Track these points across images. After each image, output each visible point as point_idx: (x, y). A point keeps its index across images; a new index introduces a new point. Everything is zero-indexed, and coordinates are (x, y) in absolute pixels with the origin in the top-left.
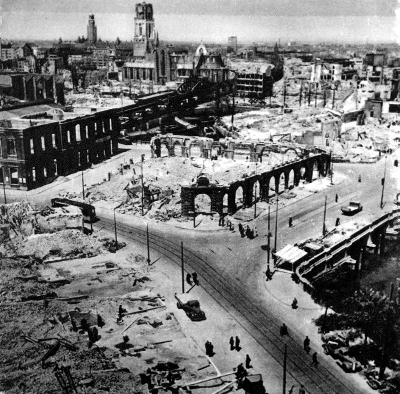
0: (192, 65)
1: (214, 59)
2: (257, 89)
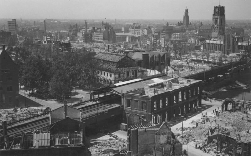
0: (247, 43)
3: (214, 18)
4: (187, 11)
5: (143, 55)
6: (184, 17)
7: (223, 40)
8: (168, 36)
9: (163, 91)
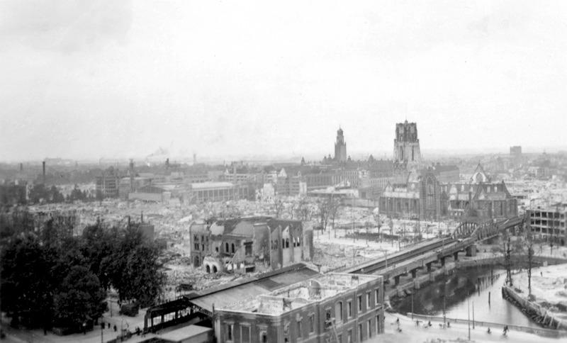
0: (468, 195)
1: (496, 188)
3: (397, 146)
4: (340, 133)
8: (305, 187)
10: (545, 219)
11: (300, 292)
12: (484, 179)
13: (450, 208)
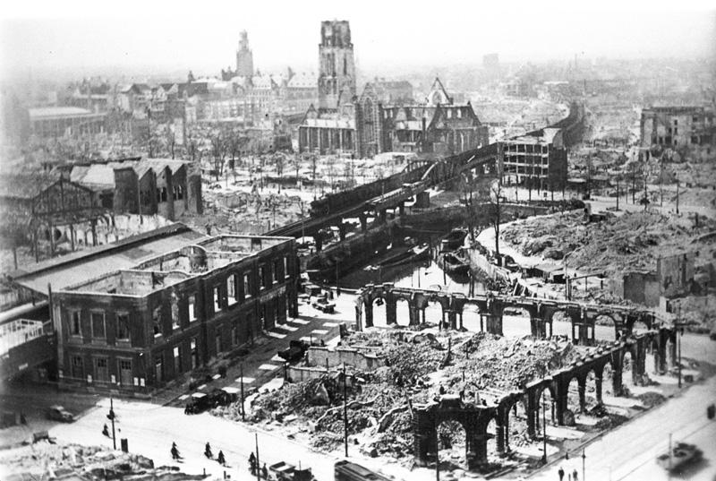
0: (421, 123)
1: (459, 112)
2: (538, 170)
3: (323, 54)
5: (116, 171)
6: (238, 56)
7: (353, 117)
9: (178, 274)
10: (522, 154)
11: (178, 263)
12: (444, 101)
13: (396, 140)
